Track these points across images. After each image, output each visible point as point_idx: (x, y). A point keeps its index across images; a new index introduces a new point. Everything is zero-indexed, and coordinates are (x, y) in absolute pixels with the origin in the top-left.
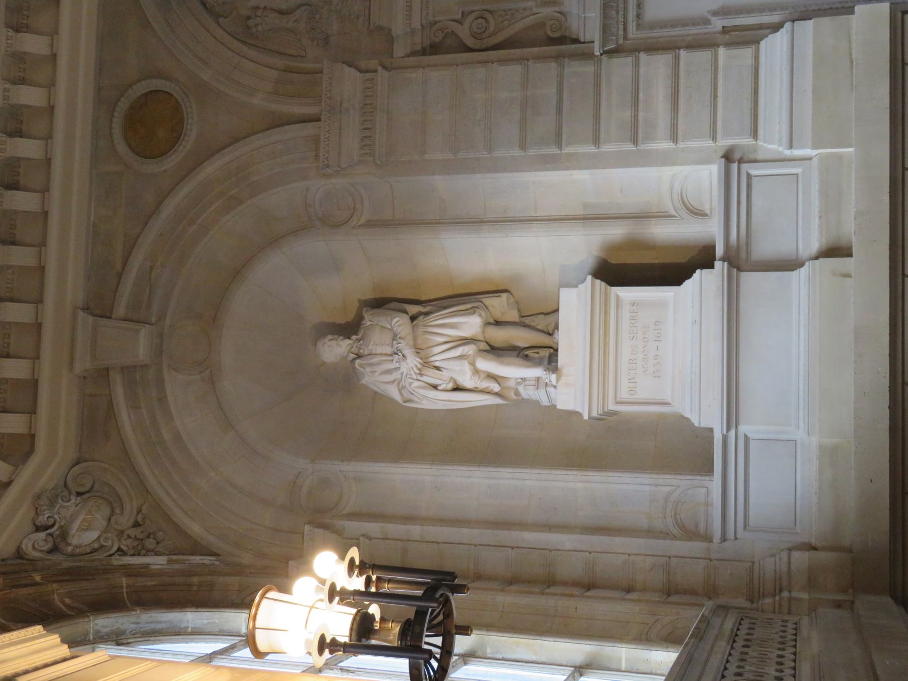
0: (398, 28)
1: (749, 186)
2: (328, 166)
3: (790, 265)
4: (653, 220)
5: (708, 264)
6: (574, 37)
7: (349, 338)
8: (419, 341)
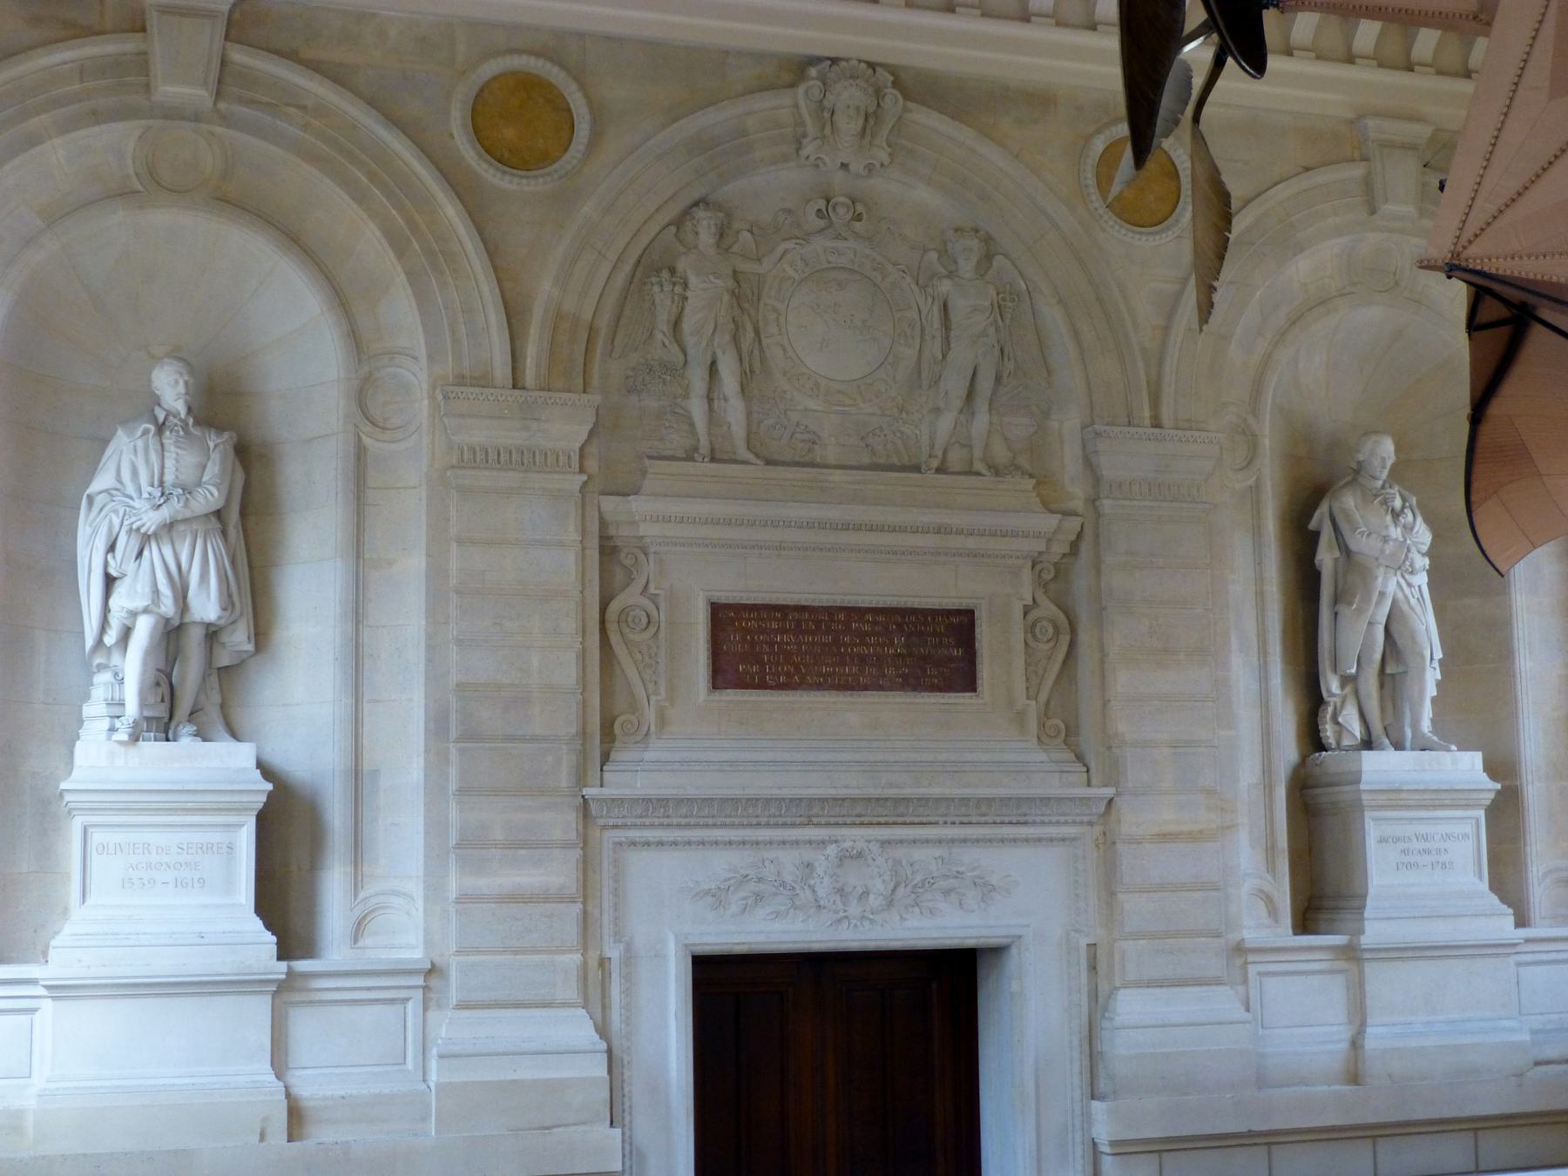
0: (638, 505)
1: (392, 1001)
2: (446, 397)
3: (279, 1059)
4: (350, 869)
5: (285, 952)
6: (613, 756)
7: (189, 410)
8: (182, 527)
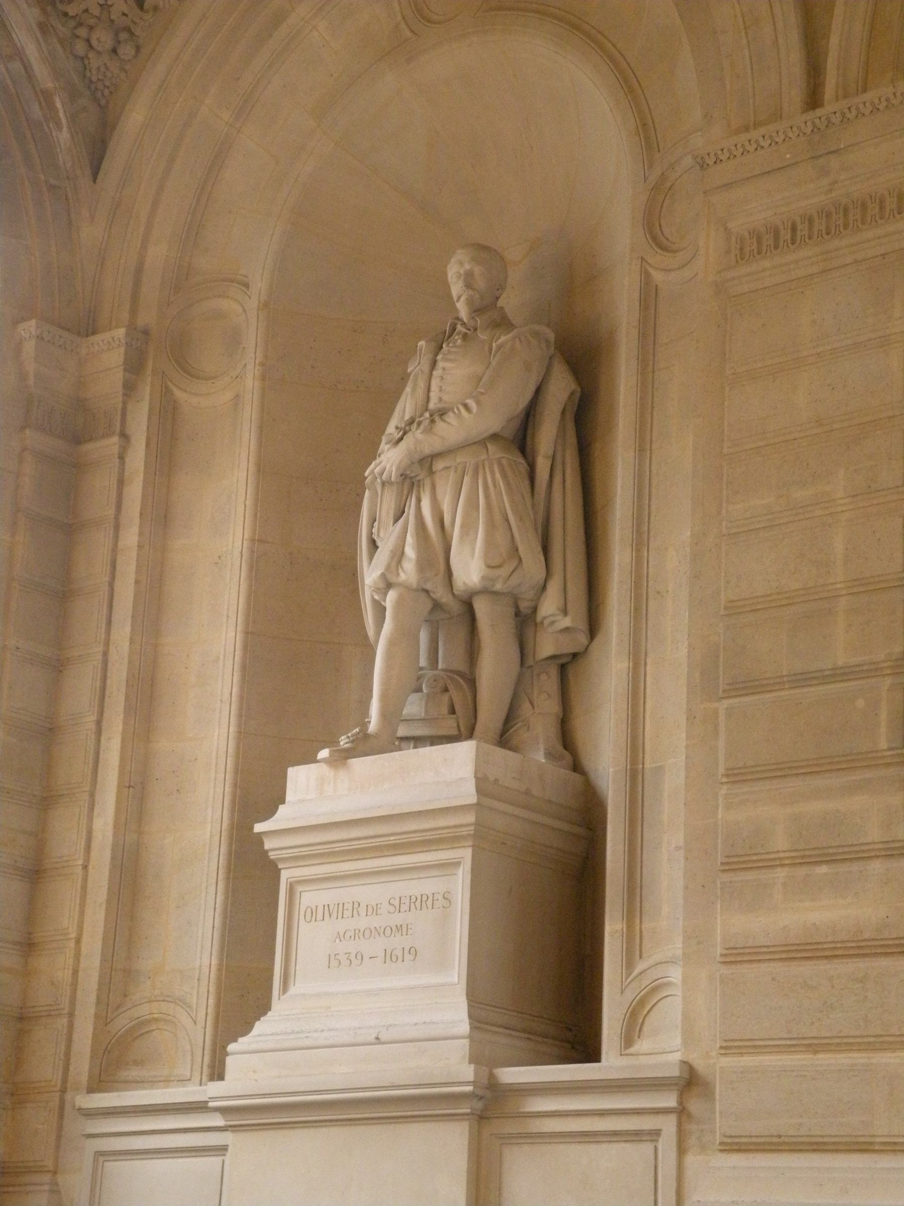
1: (635, 1136)
